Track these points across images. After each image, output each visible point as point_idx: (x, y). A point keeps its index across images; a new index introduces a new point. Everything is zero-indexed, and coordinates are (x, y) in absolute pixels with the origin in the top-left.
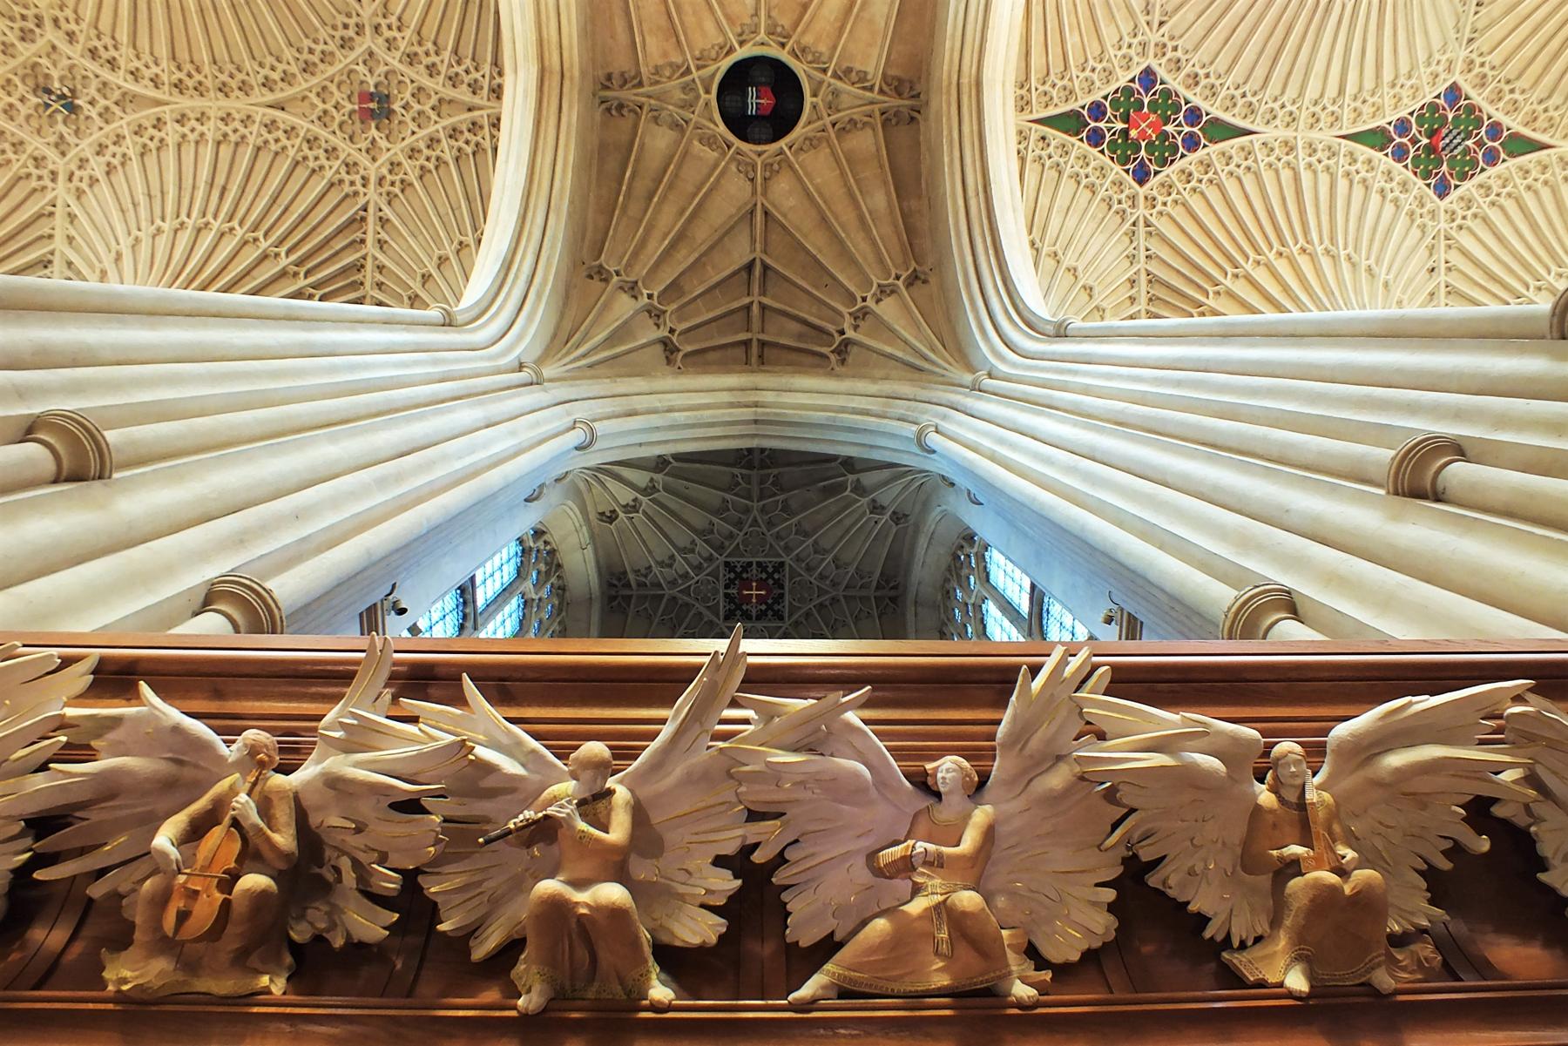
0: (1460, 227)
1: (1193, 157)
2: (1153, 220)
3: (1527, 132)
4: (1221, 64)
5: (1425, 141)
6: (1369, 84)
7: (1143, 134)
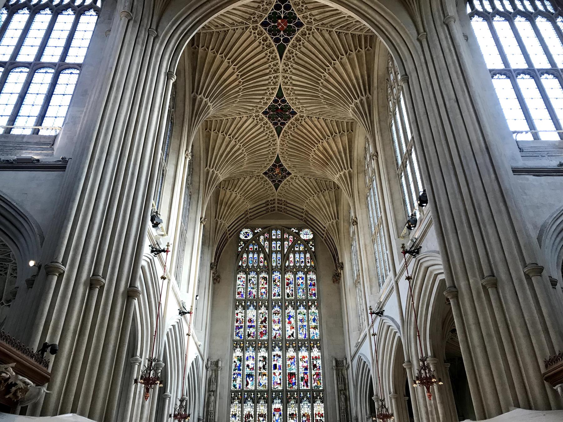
0: (254, 119)
1: (272, 41)
2: (248, 30)
3: (283, 131)
4: (303, 49)
5: (279, 107)
6: (296, 92)
7: (279, 24)
